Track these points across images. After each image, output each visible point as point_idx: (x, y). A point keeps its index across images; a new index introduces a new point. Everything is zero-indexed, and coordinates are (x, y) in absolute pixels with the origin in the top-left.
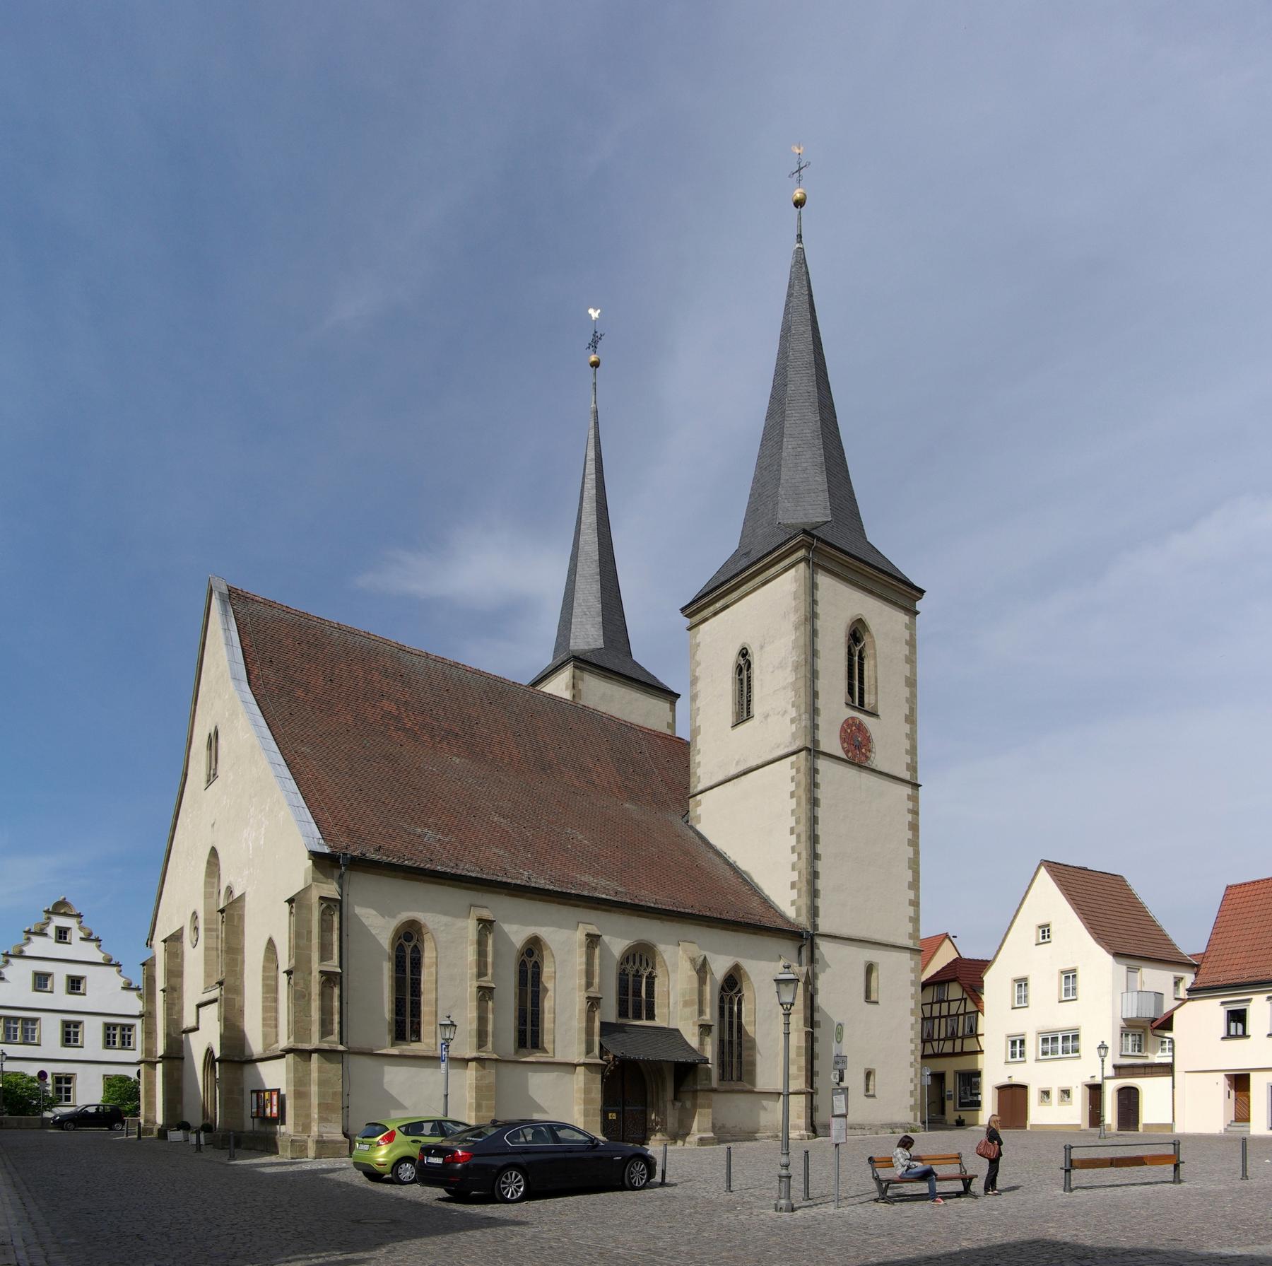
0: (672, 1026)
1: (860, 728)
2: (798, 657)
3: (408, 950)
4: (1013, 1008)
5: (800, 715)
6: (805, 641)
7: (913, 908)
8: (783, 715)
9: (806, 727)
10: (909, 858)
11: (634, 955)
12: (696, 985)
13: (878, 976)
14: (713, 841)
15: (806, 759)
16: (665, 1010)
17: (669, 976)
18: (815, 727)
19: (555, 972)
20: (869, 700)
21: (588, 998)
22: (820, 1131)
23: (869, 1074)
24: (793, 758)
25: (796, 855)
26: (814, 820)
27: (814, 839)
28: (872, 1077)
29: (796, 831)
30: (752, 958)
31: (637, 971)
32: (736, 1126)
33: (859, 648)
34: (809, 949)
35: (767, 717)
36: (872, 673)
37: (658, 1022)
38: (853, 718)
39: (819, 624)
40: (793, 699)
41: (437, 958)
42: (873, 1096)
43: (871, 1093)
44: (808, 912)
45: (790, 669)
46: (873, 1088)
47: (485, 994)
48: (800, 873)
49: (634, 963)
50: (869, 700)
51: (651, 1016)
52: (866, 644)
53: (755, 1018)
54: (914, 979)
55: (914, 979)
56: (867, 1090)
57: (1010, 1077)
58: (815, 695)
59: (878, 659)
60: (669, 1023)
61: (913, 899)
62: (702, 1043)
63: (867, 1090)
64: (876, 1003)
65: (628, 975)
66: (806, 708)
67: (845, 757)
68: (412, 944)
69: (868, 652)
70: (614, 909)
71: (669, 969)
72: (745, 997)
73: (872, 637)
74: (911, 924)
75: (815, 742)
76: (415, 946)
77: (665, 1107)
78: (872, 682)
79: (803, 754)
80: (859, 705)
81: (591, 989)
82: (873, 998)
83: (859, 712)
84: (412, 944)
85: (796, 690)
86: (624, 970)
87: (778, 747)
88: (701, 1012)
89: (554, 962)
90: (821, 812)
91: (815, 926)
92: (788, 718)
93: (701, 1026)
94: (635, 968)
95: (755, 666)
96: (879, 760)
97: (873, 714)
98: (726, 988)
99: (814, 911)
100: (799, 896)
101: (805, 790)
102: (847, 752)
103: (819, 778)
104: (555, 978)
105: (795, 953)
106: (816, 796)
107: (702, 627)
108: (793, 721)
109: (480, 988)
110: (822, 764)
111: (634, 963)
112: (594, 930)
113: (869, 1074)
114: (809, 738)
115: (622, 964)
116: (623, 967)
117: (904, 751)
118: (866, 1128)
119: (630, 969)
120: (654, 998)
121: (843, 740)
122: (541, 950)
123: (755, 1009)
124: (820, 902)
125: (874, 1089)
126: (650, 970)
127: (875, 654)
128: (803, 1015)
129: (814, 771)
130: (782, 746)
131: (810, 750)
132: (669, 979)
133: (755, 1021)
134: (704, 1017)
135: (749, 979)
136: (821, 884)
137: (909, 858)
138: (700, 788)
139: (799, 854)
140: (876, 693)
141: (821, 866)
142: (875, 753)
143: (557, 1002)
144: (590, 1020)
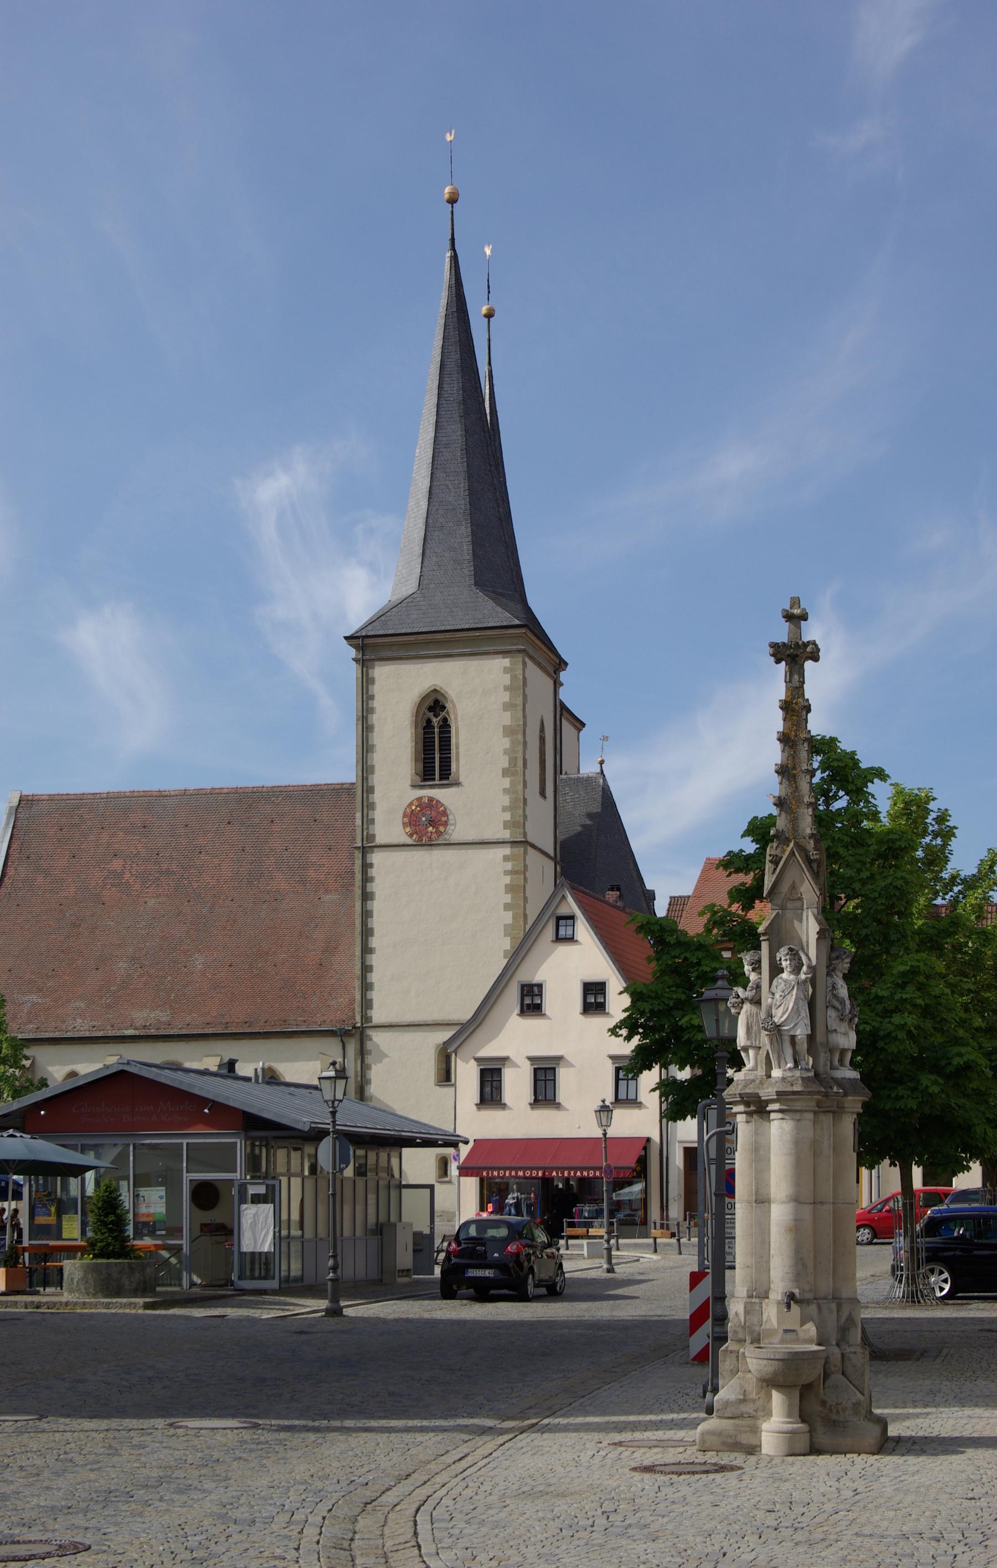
1: (432, 804)
30: (287, 1060)
38: (419, 799)
67: (409, 841)
73: (452, 702)
83: (439, 788)
91: (366, 1018)
137: (505, 925)
141: (374, 960)
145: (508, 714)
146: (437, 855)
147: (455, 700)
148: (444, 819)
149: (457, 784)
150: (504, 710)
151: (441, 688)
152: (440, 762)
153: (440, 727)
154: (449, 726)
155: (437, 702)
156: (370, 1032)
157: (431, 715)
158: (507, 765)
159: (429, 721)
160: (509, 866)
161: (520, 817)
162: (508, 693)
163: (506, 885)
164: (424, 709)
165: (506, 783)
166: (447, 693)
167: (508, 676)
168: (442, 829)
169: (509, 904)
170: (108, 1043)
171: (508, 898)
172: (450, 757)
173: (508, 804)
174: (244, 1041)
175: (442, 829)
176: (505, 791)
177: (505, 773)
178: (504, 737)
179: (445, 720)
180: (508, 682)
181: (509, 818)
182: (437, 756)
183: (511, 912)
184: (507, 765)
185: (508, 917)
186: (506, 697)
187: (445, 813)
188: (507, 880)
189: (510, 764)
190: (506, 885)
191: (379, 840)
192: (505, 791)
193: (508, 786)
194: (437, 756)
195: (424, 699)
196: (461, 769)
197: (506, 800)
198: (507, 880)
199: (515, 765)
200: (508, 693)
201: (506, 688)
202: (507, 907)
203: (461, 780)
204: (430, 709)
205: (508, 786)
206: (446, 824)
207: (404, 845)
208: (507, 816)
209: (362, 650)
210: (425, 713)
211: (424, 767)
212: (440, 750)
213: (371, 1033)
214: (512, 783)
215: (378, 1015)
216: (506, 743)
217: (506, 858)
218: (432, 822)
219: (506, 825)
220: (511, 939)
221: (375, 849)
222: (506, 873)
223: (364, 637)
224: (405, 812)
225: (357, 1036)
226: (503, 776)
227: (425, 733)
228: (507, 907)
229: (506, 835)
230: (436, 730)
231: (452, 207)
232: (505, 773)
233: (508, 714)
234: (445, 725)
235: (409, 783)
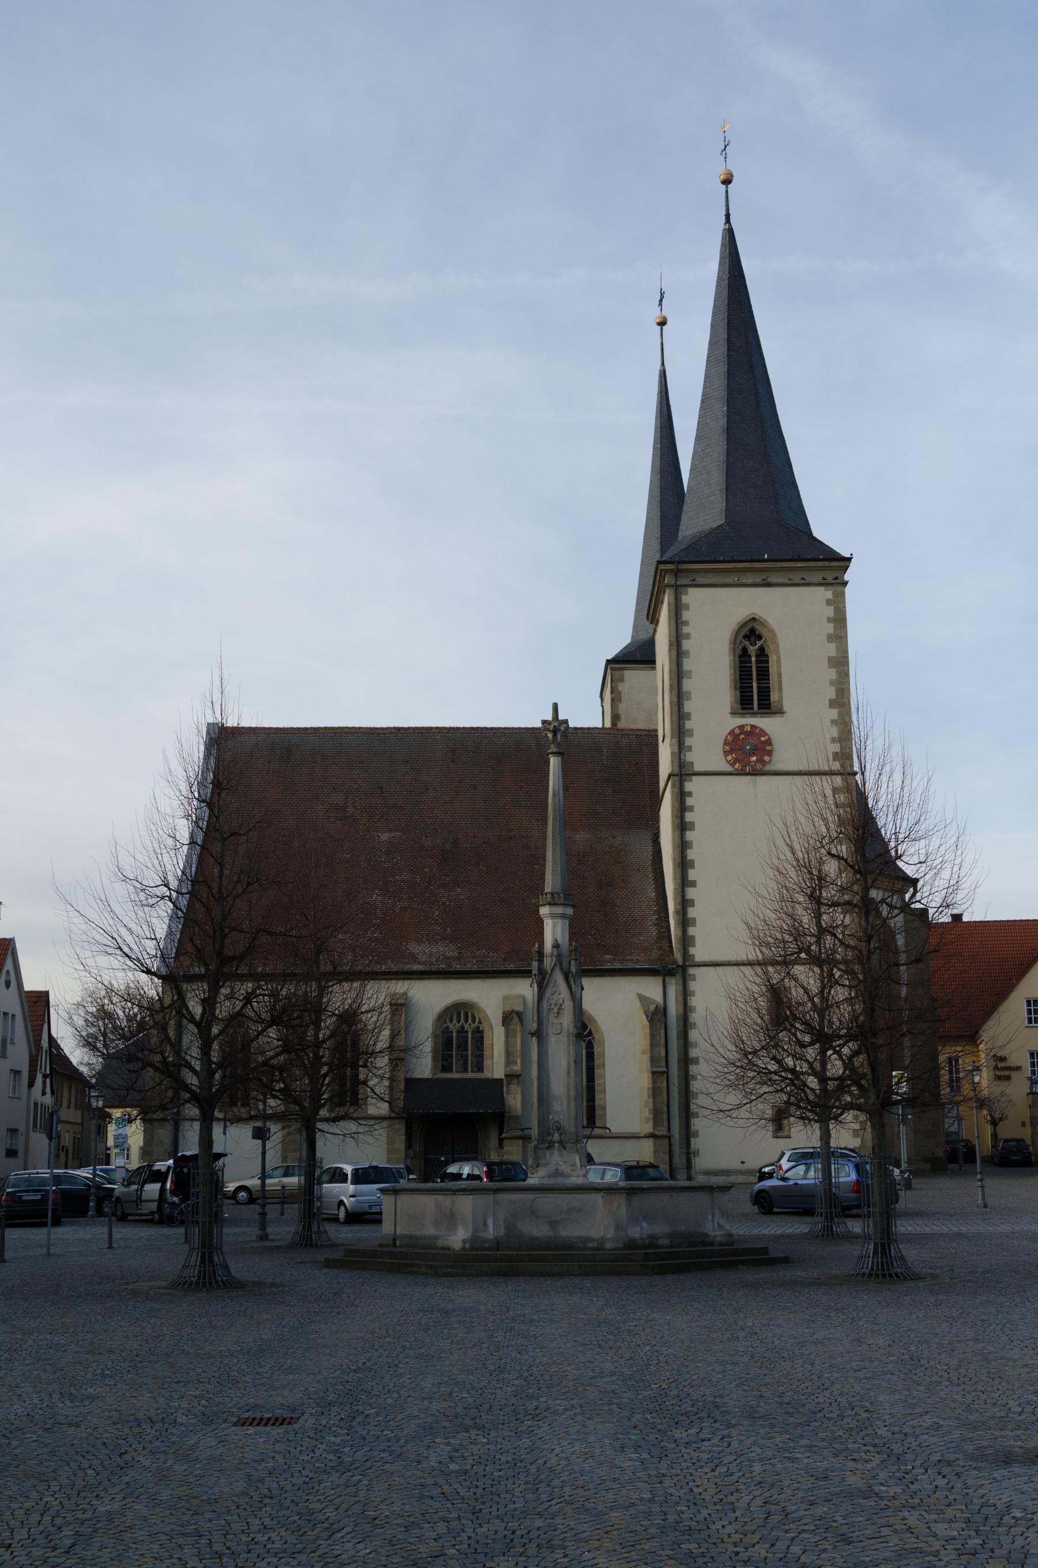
1: (754, 732)
38: (741, 727)
49: (459, 1021)
51: (480, 1068)
65: (452, 1032)
67: (729, 769)
94: (458, 1026)
96: (783, 757)
102: (733, 765)
111: (459, 1021)
126: (476, 1024)
148: (768, 748)
149: (780, 712)
151: (760, 617)
152: (758, 692)
153: (757, 656)
154: (767, 656)
155: (752, 631)
156: (692, 971)
157: (747, 643)
158: (834, 696)
159: (745, 650)
162: (832, 625)
164: (740, 638)
166: (766, 621)
167: (831, 609)
168: (766, 758)
172: (769, 688)
175: (766, 758)
179: (762, 649)
182: (755, 685)
184: (834, 696)
187: (769, 742)
189: (837, 695)
191: (697, 768)
194: (755, 685)
195: (742, 627)
200: (832, 625)
201: (829, 620)
203: (785, 709)
204: (747, 637)
206: (770, 753)
209: (676, 575)
210: (741, 642)
211: (741, 696)
212: (758, 679)
215: (699, 952)
218: (754, 751)
221: (694, 778)
224: (726, 740)
226: (830, 707)
227: (740, 662)
230: (753, 659)
231: (727, 187)
235: (729, 710)
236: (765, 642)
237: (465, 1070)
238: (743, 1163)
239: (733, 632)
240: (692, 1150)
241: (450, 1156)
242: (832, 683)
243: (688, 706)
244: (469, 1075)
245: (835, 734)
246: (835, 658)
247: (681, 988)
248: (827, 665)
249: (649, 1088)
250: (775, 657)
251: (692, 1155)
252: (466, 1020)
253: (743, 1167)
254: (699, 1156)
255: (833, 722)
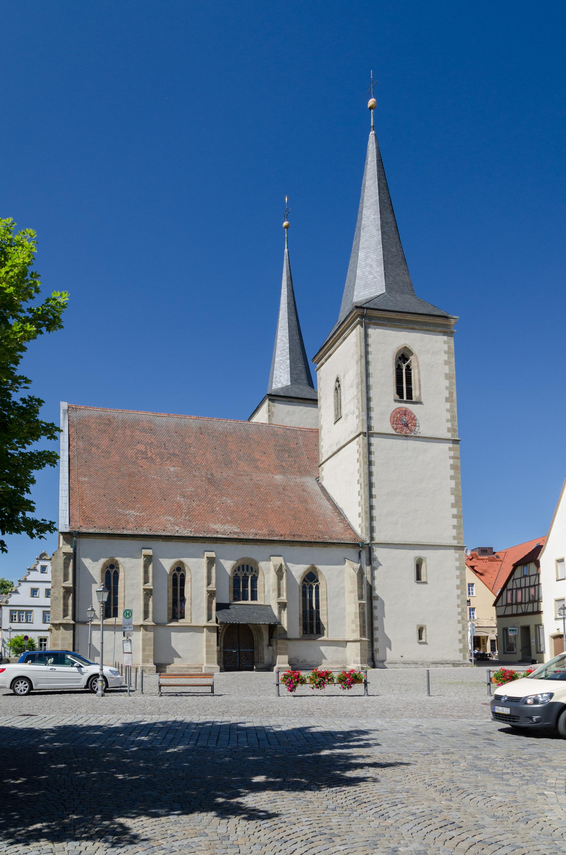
0: (267, 604)
2: (358, 380)
3: (112, 573)
4: (557, 581)
5: (360, 414)
6: (361, 369)
7: (456, 519)
8: (353, 414)
9: (362, 420)
10: (451, 488)
11: (243, 566)
12: (276, 580)
13: (426, 565)
14: (329, 491)
15: (363, 439)
16: (263, 595)
17: (264, 575)
18: (369, 418)
19: (191, 578)
20: (415, 394)
21: (207, 591)
22: (377, 664)
23: (420, 631)
24: (357, 439)
25: (360, 496)
26: (370, 474)
27: (371, 485)
28: (424, 631)
29: (360, 482)
31: (245, 574)
32: (314, 661)
33: (406, 364)
34: (368, 553)
35: (347, 416)
36: (417, 377)
37: (259, 602)
39: (370, 358)
40: (357, 405)
41: (124, 576)
42: (425, 643)
43: (423, 640)
44: (366, 530)
45: (355, 387)
46: (425, 637)
47: (148, 593)
48: (362, 507)
49: (243, 570)
50: (415, 394)
51: (254, 598)
52: (412, 360)
53: (327, 596)
54: (458, 565)
55: (458, 565)
56: (420, 638)
57: (558, 629)
58: (369, 399)
59: (421, 368)
60: (264, 602)
61: (456, 513)
62: (280, 613)
63: (420, 638)
64: (426, 583)
66: (362, 409)
67: (394, 432)
68: (114, 570)
69: (413, 366)
70: (226, 542)
71: (265, 572)
72: (321, 584)
74: (455, 530)
75: (369, 428)
76: (116, 571)
77: (263, 649)
78: (417, 382)
79: (361, 436)
80: (407, 398)
81: (210, 586)
82: (423, 579)
84: (114, 570)
85: (358, 399)
86: (236, 574)
87: (352, 433)
88: (279, 595)
89: (191, 573)
90: (374, 469)
91: (372, 538)
92: (355, 415)
93: (279, 603)
95: (342, 387)
96: (423, 429)
97: (419, 403)
98: (306, 579)
99: (372, 529)
100: (362, 522)
101: (363, 457)
102: (396, 429)
103: (373, 449)
104: (191, 581)
105: (357, 556)
106: (370, 460)
107: (322, 368)
108: (357, 417)
109: (145, 590)
110: (373, 440)
111: (243, 570)
112: (212, 555)
113: (420, 631)
114: (365, 426)
115: (235, 571)
116: (236, 573)
117: (445, 420)
118: (420, 663)
119: (241, 575)
120: (257, 588)
121: (393, 423)
122: (184, 567)
123: (327, 591)
124: (375, 524)
125: (426, 639)
127: (418, 365)
128: (357, 593)
129: (369, 445)
130: (353, 433)
131: (366, 433)
132: (264, 578)
133: (327, 598)
134: (281, 598)
135: (322, 573)
136: (375, 513)
137: (451, 488)
138: (323, 460)
139: (361, 496)
140: (420, 389)
141: (375, 502)
142: (419, 426)
143: (192, 594)
144: (210, 603)
145: (447, 367)
146: (411, 443)
147: (417, 354)
150: (445, 364)
151: (409, 346)
158: (448, 396)
160: (452, 454)
161: (456, 426)
163: (451, 465)
165: (448, 406)
169: (452, 476)
170: (205, 543)
171: (452, 473)
173: (449, 418)
174: (295, 547)
176: (448, 410)
177: (447, 400)
178: (445, 379)
180: (446, 349)
181: (450, 426)
183: (454, 481)
185: (452, 484)
186: (445, 357)
188: (451, 462)
189: (449, 395)
190: (451, 465)
192: (448, 410)
193: (449, 408)
195: (399, 351)
196: (422, 395)
197: (448, 416)
198: (451, 462)
199: (452, 397)
202: (452, 478)
203: (422, 401)
205: (449, 408)
207: (392, 435)
208: (449, 425)
213: (374, 548)
214: (451, 406)
216: (447, 383)
217: (450, 449)
219: (449, 430)
220: (455, 496)
222: (451, 458)
223: (367, 308)
225: (367, 549)
226: (446, 401)
228: (452, 478)
229: (449, 436)
232: (447, 400)
233: (447, 367)
234: (408, 369)
236: (411, 362)
237: (247, 599)
238: (402, 656)
239: (395, 353)
240: (374, 649)
241: (237, 650)
242: (447, 388)
243: (372, 394)
244: (249, 602)
245: (449, 417)
246: (449, 374)
247: (368, 556)
248: (444, 378)
249: (356, 613)
250: (416, 371)
251: (375, 652)
252: (247, 570)
253: (402, 659)
254: (378, 652)
255: (448, 410)
